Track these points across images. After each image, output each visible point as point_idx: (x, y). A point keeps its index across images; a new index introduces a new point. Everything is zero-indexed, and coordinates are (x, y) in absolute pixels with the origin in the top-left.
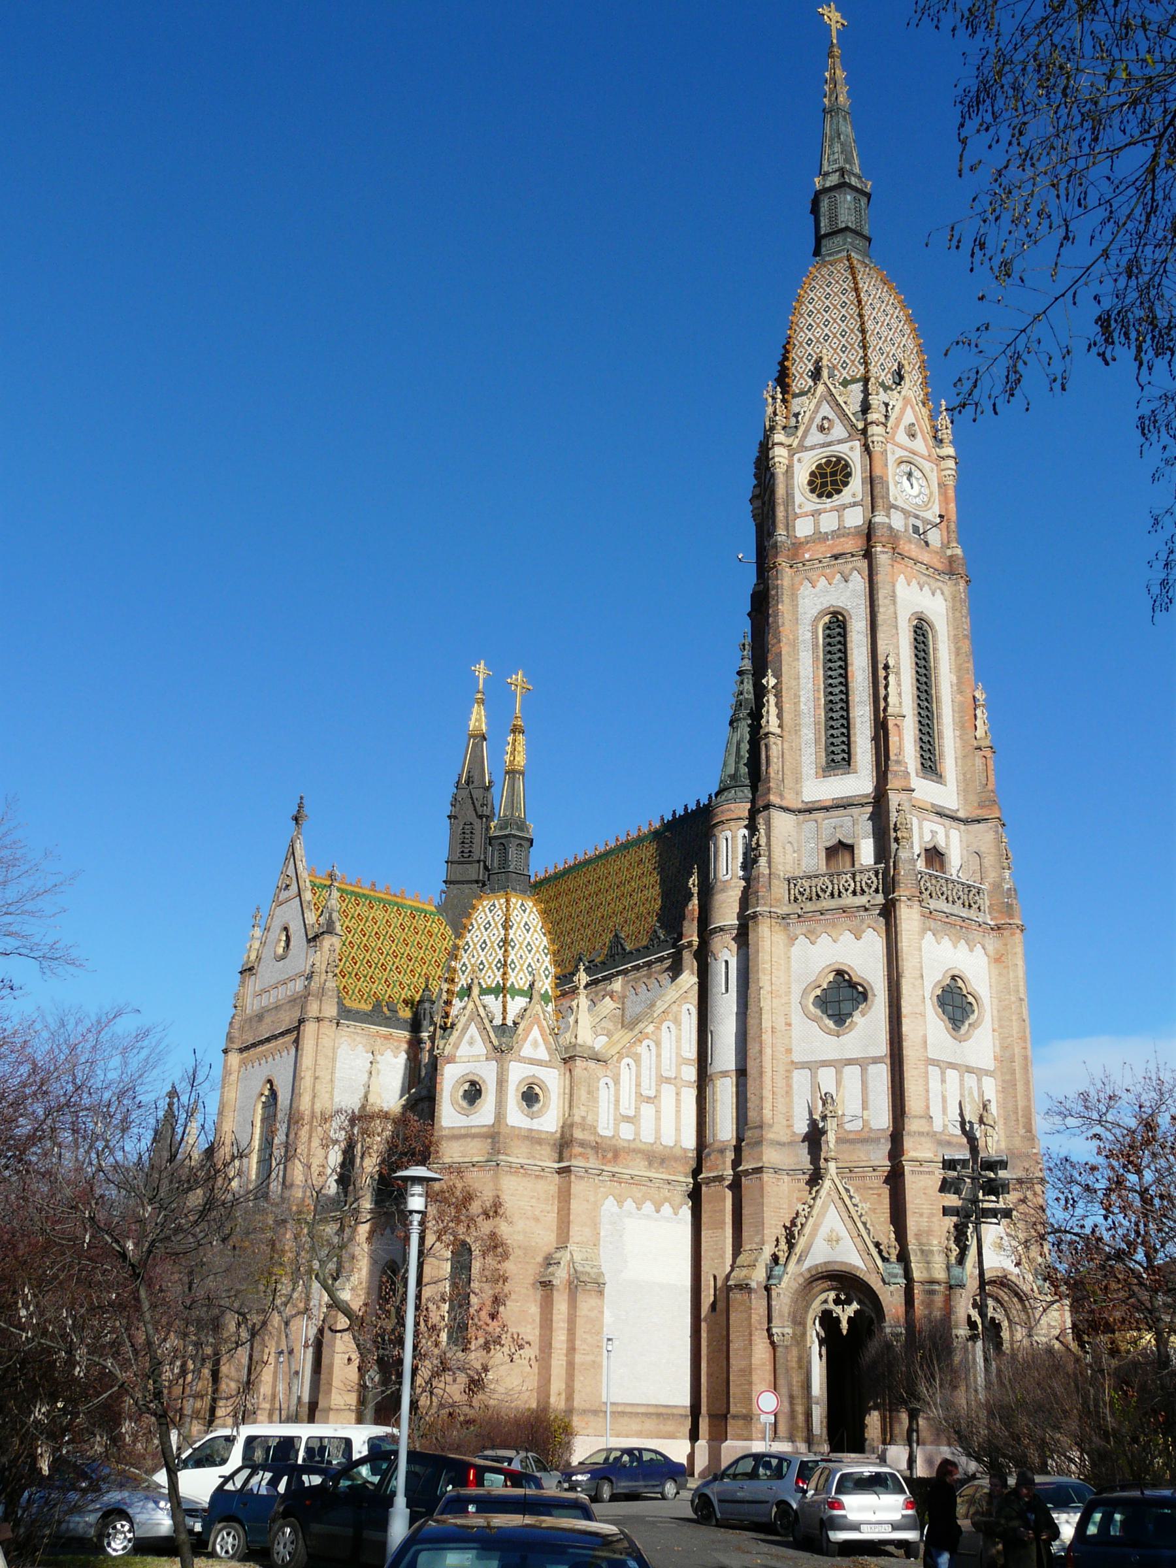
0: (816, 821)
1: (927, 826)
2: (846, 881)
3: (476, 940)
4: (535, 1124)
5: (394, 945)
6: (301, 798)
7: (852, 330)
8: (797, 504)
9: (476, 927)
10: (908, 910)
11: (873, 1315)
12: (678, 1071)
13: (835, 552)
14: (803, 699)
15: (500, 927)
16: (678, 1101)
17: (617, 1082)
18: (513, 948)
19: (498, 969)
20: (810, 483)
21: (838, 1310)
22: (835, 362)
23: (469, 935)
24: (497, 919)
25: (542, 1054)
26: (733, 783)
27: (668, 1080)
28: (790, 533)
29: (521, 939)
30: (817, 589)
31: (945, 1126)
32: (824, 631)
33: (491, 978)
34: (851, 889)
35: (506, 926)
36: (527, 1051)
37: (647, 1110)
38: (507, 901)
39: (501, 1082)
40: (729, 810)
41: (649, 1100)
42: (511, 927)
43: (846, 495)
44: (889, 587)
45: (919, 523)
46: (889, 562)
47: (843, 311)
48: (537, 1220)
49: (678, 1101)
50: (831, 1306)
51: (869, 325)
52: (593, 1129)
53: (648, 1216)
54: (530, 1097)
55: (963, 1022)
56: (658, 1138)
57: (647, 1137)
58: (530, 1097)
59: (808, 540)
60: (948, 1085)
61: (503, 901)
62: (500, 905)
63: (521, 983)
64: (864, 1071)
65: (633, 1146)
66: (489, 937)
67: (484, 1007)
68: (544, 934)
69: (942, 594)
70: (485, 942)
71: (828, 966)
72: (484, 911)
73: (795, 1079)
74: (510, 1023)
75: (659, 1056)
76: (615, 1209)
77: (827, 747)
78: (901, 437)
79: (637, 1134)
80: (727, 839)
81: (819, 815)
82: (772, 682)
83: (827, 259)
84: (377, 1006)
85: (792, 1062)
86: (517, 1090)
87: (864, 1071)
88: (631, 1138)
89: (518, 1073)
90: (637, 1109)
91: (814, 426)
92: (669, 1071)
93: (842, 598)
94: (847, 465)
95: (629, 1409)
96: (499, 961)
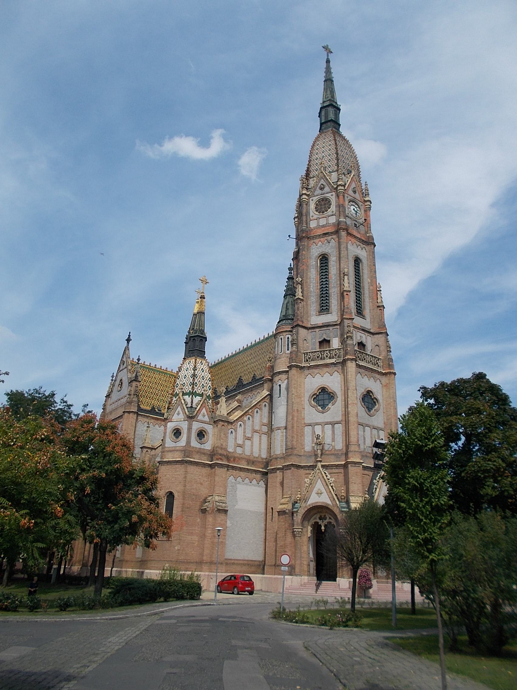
0: (315, 331)
1: (359, 334)
2: (327, 353)
3: (182, 375)
4: (202, 447)
5: (162, 387)
6: (130, 333)
7: (333, 154)
8: (311, 216)
9: (183, 370)
10: (351, 363)
11: (335, 524)
12: (261, 428)
13: (325, 232)
14: (311, 286)
15: (192, 369)
16: (260, 439)
17: (236, 431)
18: (196, 377)
19: (190, 386)
20: (316, 208)
21: (320, 522)
22: (326, 165)
23: (180, 373)
24: (191, 366)
25: (206, 419)
26: (284, 318)
27: (256, 431)
28: (308, 226)
29: (200, 374)
30: (318, 246)
31: (365, 449)
32: (320, 261)
33: (188, 389)
34: (329, 356)
35: (195, 369)
36: (200, 417)
37: (248, 443)
38: (196, 360)
39: (190, 429)
40: (283, 328)
41: (248, 439)
42: (196, 370)
43: (330, 212)
44: (345, 244)
45: (356, 223)
46: (346, 235)
47: (330, 147)
48: (202, 484)
49: (260, 439)
50: (318, 520)
51: (339, 152)
52: (226, 450)
53: (246, 484)
54: (201, 434)
55: (372, 409)
56: (252, 453)
57: (248, 453)
58: (201, 434)
59: (315, 228)
60: (366, 433)
61: (194, 360)
62: (192, 361)
63: (199, 391)
64: (333, 427)
66: (187, 374)
67: (184, 400)
68: (209, 373)
70: (186, 375)
71: (319, 386)
72: (186, 364)
73: (305, 430)
74: (194, 406)
75: (253, 421)
76: (234, 481)
77: (320, 304)
78: (350, 192)
79: (244, 451)
80: (281, 339)
81: (317, 330)
82: (301, 279)
83: (324, 131)
84: (153, 408)
85: (305, 423)
86: (195, 432)
87: (333, 427)
88: (241, 453)
89: (196, 426)
90: (244, 441)
91: (318, 187)
92: (257, 428)
93: (327, 249)
94: (329, 201)
95: (236, 562)
96: (191, 382)
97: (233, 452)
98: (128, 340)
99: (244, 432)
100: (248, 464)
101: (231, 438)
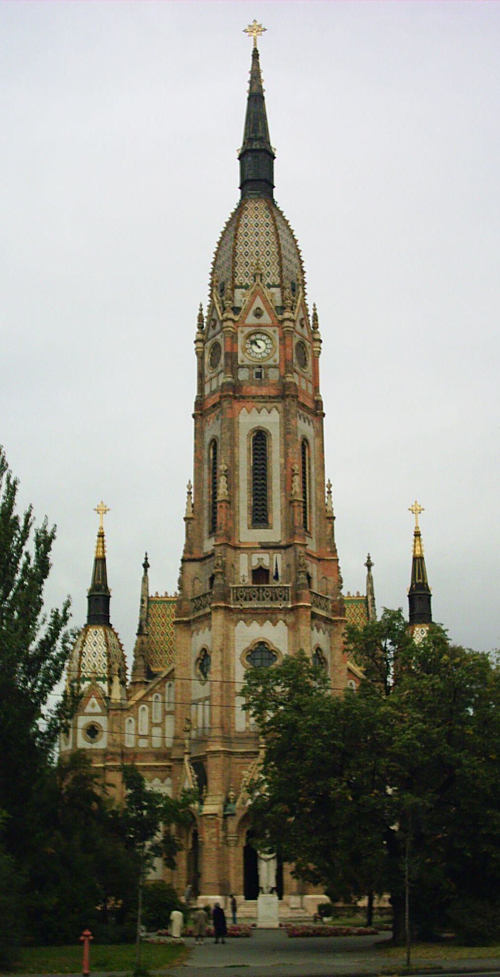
4: (94, 746)
6: (146, 554)
17: (136, 719)
25: (98, 709)
36: (88, 709)
37: (157, 731)
41: (157, 725)
56: (164, 743)
57: (157, 743)
65: (147, 750)
69: (277, 409)
78: (251, 319)
79: (150, 744)
97: (134, 748)
98: (146, 566)
99: (150, 718)
100: (157, 759)
101: (130, 728)
